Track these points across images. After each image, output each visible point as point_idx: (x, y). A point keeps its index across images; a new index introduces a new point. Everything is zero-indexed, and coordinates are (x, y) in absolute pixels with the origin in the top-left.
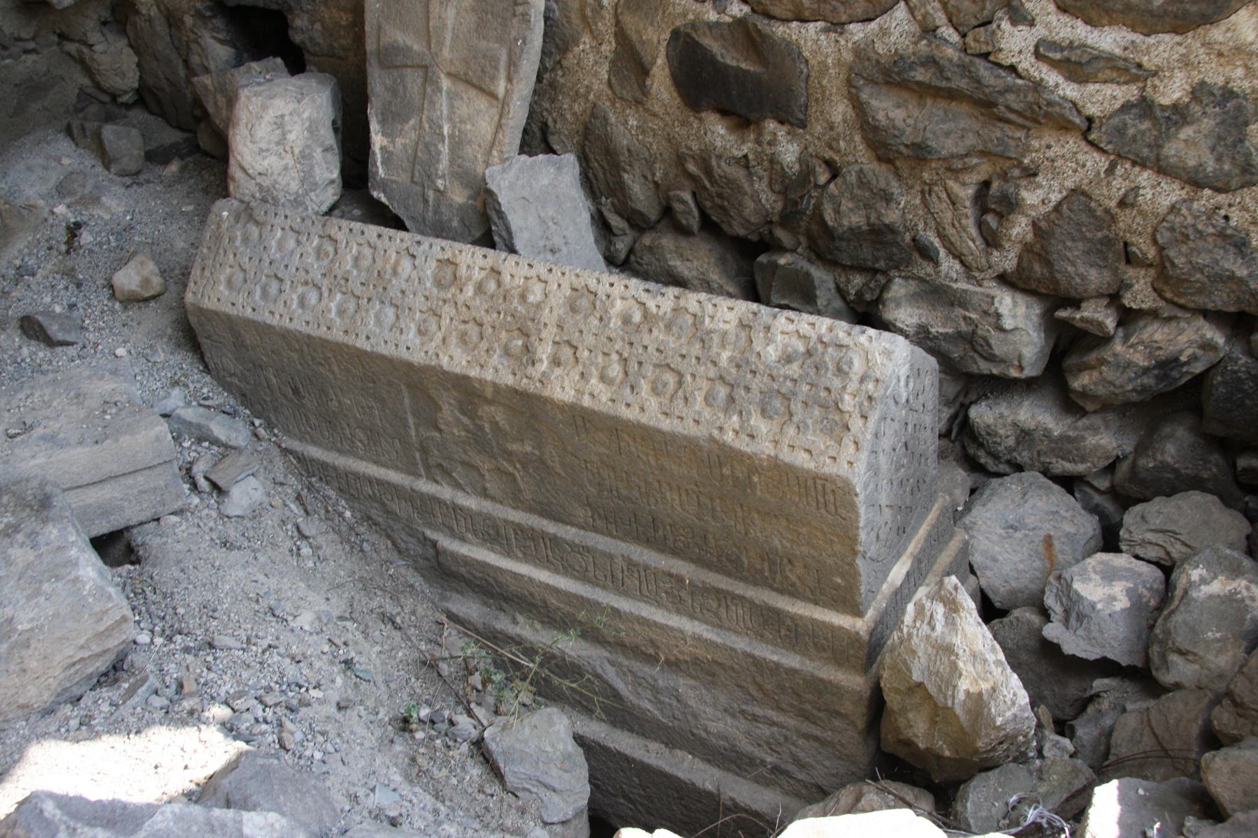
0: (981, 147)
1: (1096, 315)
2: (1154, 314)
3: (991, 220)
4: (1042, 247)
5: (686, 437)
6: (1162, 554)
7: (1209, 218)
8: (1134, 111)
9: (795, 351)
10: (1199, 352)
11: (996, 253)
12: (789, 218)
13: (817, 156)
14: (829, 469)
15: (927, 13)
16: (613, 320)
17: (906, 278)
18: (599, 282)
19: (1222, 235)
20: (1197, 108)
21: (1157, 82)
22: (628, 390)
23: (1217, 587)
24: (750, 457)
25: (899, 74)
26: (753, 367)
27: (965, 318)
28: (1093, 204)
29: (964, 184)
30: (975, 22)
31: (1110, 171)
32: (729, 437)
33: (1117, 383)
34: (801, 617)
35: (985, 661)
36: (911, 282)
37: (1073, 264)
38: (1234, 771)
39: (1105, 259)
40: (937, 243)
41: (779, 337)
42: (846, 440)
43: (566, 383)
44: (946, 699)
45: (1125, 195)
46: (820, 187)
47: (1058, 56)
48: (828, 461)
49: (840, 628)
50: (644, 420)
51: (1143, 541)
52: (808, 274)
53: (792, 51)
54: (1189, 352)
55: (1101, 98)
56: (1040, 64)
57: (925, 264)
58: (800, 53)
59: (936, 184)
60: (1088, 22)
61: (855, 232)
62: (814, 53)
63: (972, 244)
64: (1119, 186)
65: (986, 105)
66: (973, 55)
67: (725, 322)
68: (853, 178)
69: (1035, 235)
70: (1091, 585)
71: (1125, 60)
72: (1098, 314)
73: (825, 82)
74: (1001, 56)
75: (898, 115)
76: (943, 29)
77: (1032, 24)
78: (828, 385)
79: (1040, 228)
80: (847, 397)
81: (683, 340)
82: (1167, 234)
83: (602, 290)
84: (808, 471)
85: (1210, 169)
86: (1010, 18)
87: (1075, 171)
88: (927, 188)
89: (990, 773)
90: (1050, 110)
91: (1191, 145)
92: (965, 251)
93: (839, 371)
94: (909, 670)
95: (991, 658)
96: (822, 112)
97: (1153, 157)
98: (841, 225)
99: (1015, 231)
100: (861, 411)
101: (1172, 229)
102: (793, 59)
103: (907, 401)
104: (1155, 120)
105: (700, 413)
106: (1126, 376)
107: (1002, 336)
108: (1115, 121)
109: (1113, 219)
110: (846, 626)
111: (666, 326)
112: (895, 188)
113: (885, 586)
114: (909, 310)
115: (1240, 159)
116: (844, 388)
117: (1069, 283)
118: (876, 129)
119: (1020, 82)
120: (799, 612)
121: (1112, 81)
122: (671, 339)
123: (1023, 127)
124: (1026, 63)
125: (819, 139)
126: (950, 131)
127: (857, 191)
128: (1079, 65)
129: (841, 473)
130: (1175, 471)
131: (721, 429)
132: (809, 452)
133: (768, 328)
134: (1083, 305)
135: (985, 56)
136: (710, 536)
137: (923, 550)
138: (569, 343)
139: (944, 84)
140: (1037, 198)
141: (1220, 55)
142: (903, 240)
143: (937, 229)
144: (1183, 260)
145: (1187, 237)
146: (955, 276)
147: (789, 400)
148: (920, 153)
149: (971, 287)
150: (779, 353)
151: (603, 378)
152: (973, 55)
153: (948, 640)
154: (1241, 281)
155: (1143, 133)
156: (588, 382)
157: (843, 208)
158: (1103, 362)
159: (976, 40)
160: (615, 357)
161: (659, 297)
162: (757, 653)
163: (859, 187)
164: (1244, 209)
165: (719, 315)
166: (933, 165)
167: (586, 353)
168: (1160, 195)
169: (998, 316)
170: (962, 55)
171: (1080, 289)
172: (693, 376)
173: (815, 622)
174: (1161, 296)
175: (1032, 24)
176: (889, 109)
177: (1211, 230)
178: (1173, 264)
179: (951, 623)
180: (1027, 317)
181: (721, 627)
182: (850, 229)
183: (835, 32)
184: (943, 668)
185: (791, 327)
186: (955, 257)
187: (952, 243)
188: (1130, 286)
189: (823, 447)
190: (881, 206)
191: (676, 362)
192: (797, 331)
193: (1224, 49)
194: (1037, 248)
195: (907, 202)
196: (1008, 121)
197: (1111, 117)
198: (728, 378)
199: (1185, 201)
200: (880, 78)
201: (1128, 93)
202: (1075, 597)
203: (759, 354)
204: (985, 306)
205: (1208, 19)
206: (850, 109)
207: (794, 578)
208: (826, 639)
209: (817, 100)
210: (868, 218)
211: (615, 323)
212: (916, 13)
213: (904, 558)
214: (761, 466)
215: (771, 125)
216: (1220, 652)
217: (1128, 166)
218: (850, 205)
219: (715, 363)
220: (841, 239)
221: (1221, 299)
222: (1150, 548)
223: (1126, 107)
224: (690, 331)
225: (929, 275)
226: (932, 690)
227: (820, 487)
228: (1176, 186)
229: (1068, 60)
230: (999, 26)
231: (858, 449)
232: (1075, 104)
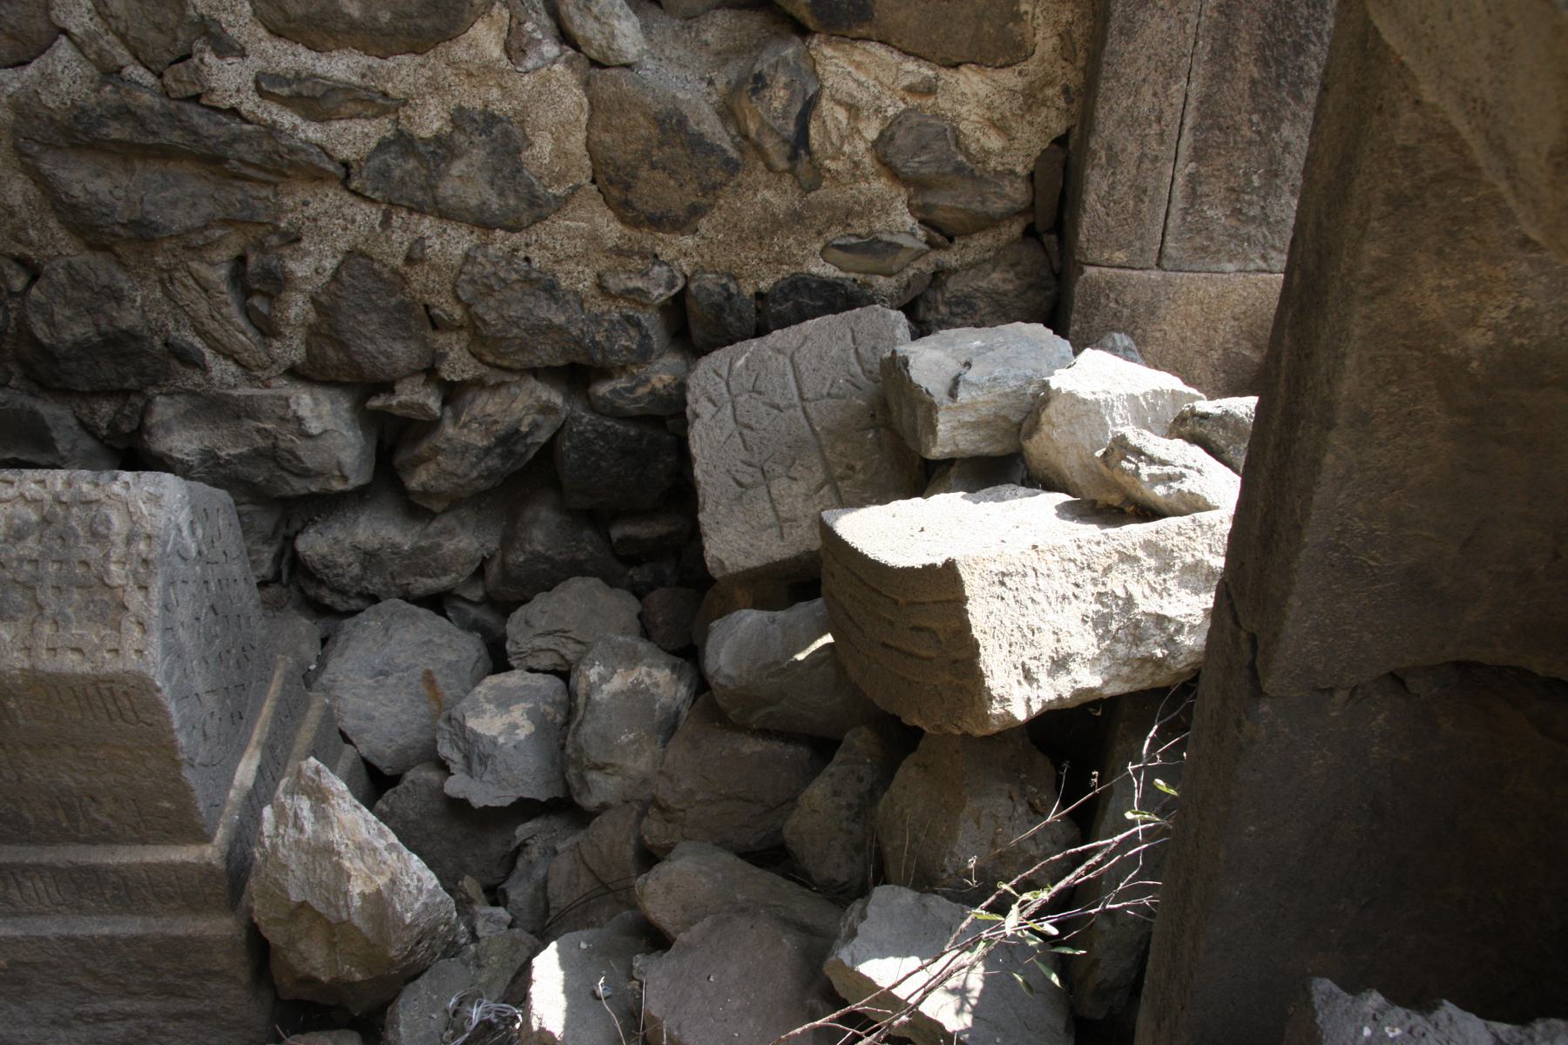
0: (221, 215)
1: (416, 397)
2: (479, 384)
3: (257, 301)
6: (557, 660)
7: (509, 263)
9: (26, 522)
10: (540, 418)
11: (276, 344)
14: (112, 665)
15: (101, 49)
17: (170, 394)
19: (527, 280)
20: (462, 138)
21: (410, 112)
23: (618, 683)
25: (86, 134)
27: (259, 431)
28: (376, 266)
29: (212, 264)
30: (168, 57)
31: (386, 222)
33: (460, 472)
34: (128, 866)
35: (375, 850)
36: (177, 398)
37: (372, 341)
38: (669, 889)
39: (408, 328)
40: (198, 343)
42: (125, 624)
45: (411, 249)
46: (17, 294)
47: (285, 91)
48: (108, 656)
49: (185, 864)
52: (33, 413)
54: (528, 420)
55: (353, 137)
57: (189, 372)
59: (176, 269)
61: (83, 347)
63: (244, 337)
64: (400, 240)
65: (213, 161)
68: (61, 276)
69: (318, 313)
70: (487, 717)
71: (367, 89)
72: (416, 395)
74: (214, 97)
75: (101, 186)
76: (130, 69)
77: (243, 54)
78: (84, 557)
79: (321, 304)
80: (113, 567)
82: (469, 288)
84: (84, 677)
85: (495, 206)
86: (213, 49)
88: (165, 276)
89: (419, 981)
90: (294, 158)
91: (465, 180)
92: (236, 347)
93: (95, 536)
94: (284, 890)
95: (380, 844)
97: (429, 200)
99: (292, 313)
101: (473, 282)
103: (200, 553)
104: (418, 156)
106: (466, 462)
107: (311, 443)
108: (375, 163)
109: (405, 279)
110: (192, 859)
112: (123, 281)
113: (232, 793)
114: (185, 435)
115: (523, 191)
116: (107, 556)
118: (74, 208)
119: (248, 127)
120: (125, 860)
121: (358, 116)
124: (248, 103)
126: (179, 199)
128: (317, 101)
129: (129, 667)
130: (548, 559)
132: (78, 650)
134: (398, 387)
135: (196, 99)
137: (273, 733)
139: (151, 140)
140: (309, 266)
141: (470, 75)
142: (153, 347)
144: (494, 315)
145: (491, 287)
146: (232, 381)
147: (33, 588)
148: (144, 233)
149: (256, 392)
153: (323, 838)
157: (58, 318)
158: (437, 451)
159: (176, 80)
162: (77, 932)
163: (73, 288)
164: (543, 247)
166: (166, 245)
168: (451, 243)
169: (299, 420)
170: (165, 101)
173: (148, 867)
174: (481, 360)
176: (84, 180)
177: (514, 276)
178: (484, 321)
179: (322, 816)
180: (335, 414)
181: (16, 914)
182: (75, 343)
184: (326, 875)
187: (217, 341)
188: (445, 355)
189: (96, 640)
190: (110, 307)
192: (22, 495)
193: (473, 69)
194: (325, 329)
195: (144, 298)
197: (368, 160)
199: (478, 247)
202: (472, 737)
206: (30, 186)
207: (105, 820)
208: (169, 884)
210: (97, 326)
212: (87, 51)
213: (250, 750)
216: (637, 754)
217: (404, 214)
218: (68, 313)
221: (546, 354)
222: (542, 655)
223: (383, 145)
225: (199, 385)
226: (320, 906)
227: (107, 693)
228: (464, 230)
229: (299, 95)
230: (202, 60)
231: (145, 632)
232: (323, 148)
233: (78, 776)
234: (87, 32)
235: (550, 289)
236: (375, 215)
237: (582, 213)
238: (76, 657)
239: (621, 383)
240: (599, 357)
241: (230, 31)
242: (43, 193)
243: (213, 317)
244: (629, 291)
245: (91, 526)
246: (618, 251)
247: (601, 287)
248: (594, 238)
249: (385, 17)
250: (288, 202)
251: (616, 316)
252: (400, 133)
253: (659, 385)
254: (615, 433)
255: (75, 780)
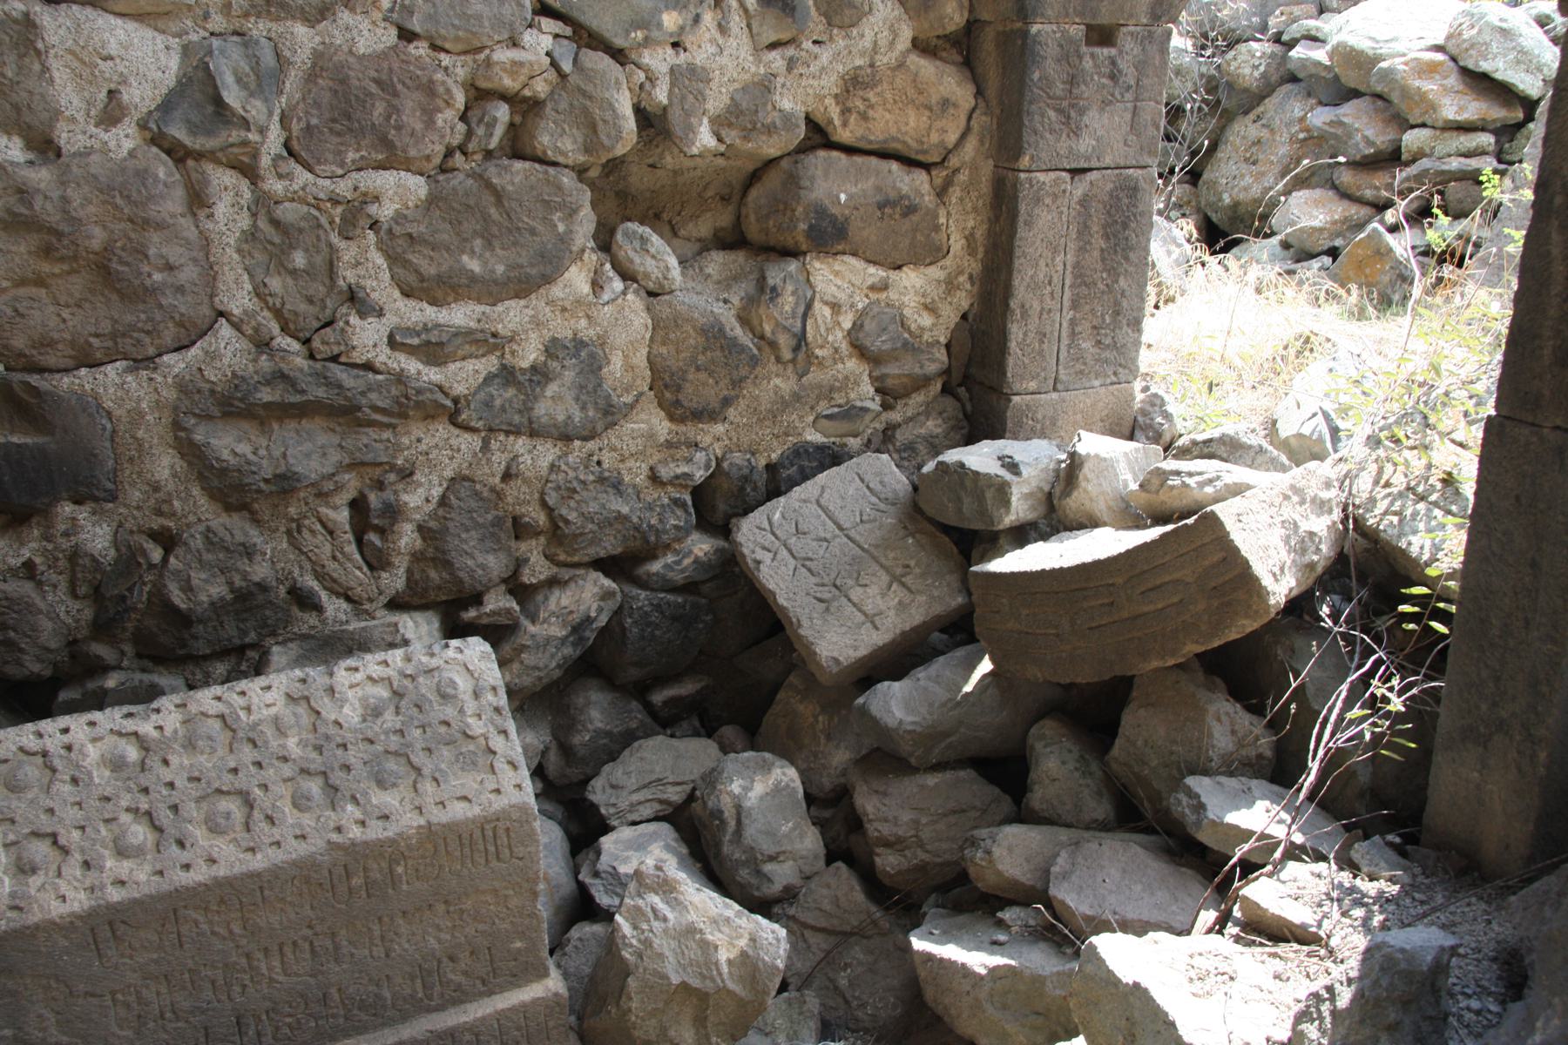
0: (347, 461)
2: (553, 582)
3: (373, 537)
4: (436, 549)
5: (294, 864)
6: (657, 806)
7: (586, 467)
8: (496, 381)
9: (381, 699)
11: (384, 575)
12: (102, 628)
13: (141, 532)
14: (499, 803)
15: (259, 324)
16: (95, 774)
18: (40, 735)
19: (601, 480)
21: (515, 347)
22: (175, 848)
23: (759, 788)
24: (392, 842)
25: (241, 400)
26: (339, 740)
28: (478, 487)
29: (335, 508)
30: (316, 325)
31: (486, 447)
32: (355, 832)
34: (483, 1018)
35: (728, 920)
36: (290, 645)
38: (1010, 849)
39: (499, 541)
40: (314, 584)
41: (350, 694)
43: (64, 888)
44: (713, 980)
45: (508, 468)
47: (416, 341)
48: (492, 797)
49: (535, 1001)
50: (221, 871)
51: (632, 805)
53: (90, 405)
54: (595, 606)
55: (464, 375)
56: (397, 354)
57: (306, 616)
58: (99, 406)
60: (434, 302)
61: (217, 607)
62: (120, 402)
63: (356, 575)
64: (499, 460)
65: (346, 414)
66: (325, 360)
67: (268, 706)
68: (198, 542)
69: (424, 539)
71: (482, 331)
73: (140, 434)
75: (244, 448)
76: (279, 339)
77: (380, 313)
78: (442, 718)
79: (430, 529)
80: (470, 720)
81: (220, 753)
82: (554, 494)
83: (54, 744)
87: (451, 458)
88: (294, 525)
91: (557, 402)
93: (444, 697)
94: (665, 977)
95: (729, 913)
96: (139, 474)
97: (525, 421)
98: (200, 603)
99: (403, 542)
100: (496, 727)
101: (558, 488)
102: (90, 415)
104: (518, 385)
105: (300, 826)
109: (499, 495)
111: (184, 747)
112: (255, 536)
115: (601, 402)
116: (461, 711)
117: (472, 577)
118: (224, 472)
119: (380, 377)
120: (479, 1014)
121: (471, 356)
122: (202, 758)
123: (394, 427)
124: (383, 356)
125: (138, 508)
126: (310, 451)
127: (208, 557)
128: (434, 350)
129: (514, 801)
130: (608, 734)
131: (339, 829)
132: (465, 798)
133: (331, 691)
134: (486, 598)
135: (334, 359)
136: (333, 991)
138: (36, 834)
139: (297, 398)
140: (418, 498)
141: (564, 310)
143: (314, 570)
144: (575, 514)
145: (574, 491)
146: (344, 618)
148: (285, 484)
149: (363, 624)
150: (360, 711)
151: (122, 852)
152: (325, 360)
154: (626, 518)
155: (511, 402)
156: (101, 869)
157: (195, 582)
158: (523, 648)
159: (323, 343)
160: (126, 818)
161: (154, 717)
163: (208, 551)
164: (614, 449)
165: (255, 700)
166: (302, 494)
167: (76, 834)
168: (537, 457)
170: (311, 362)
171: (484, 580)
172: (265, 787)
173: (500, 1015)
175: (380, 313)
176: (229, 444)
178: (567, 522)
182: (212, 604)
183: (146, 369)
184: (694, 953)
185: (359, 676)
186: (338, 595)
187: (335, 581)
188: (527, 560)
189: (476, 786)
191: (227, 782)
192: (370, 678)
193: (567, 304)
195: (274, 549)
196: (372, 424)
198: (312, 767)
199: (560, 457)
200: (216, 412)
201: (489, 364)
203: (337, 723)
204: (389, 638)
205: (548, 280)
209: (131, 460)
210: (230, 583)
211: (101, 777)
212: (245, 327)
214: (409, 847)
215: (67, 508)
216: (802, 836)
218: (203, 576)
219: (285, 759)
220: (200, 621)
221: (610, 545)
222: (641, 808)
223: (489, 379)
224: (223, 737)
225: (313, 627)
226: (695, 982)
229: (428, 343)
230: (347, 323)
232: (440, 388)
233: (443, 936)
234: (245, 312)
235: (617, 486)
236: (475, 441)
237: (643, 416)
238: (464, 804)
239: (670, 558)
240: (653, 538)
241: (373, 295)
242: (190, 464)
243: (334, 558)
244: (677, 477)
245: (438, 691)
246: (669, 445)
247: (654, 478)
248: (651, 436)
249: (500, 269)
250: (405, 441)
251: (666, 501)
252: (504, 367)
253: (701, 554)
254: (668, 603)
255: (439, 941)
